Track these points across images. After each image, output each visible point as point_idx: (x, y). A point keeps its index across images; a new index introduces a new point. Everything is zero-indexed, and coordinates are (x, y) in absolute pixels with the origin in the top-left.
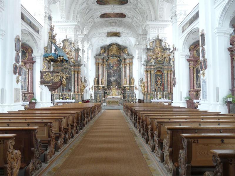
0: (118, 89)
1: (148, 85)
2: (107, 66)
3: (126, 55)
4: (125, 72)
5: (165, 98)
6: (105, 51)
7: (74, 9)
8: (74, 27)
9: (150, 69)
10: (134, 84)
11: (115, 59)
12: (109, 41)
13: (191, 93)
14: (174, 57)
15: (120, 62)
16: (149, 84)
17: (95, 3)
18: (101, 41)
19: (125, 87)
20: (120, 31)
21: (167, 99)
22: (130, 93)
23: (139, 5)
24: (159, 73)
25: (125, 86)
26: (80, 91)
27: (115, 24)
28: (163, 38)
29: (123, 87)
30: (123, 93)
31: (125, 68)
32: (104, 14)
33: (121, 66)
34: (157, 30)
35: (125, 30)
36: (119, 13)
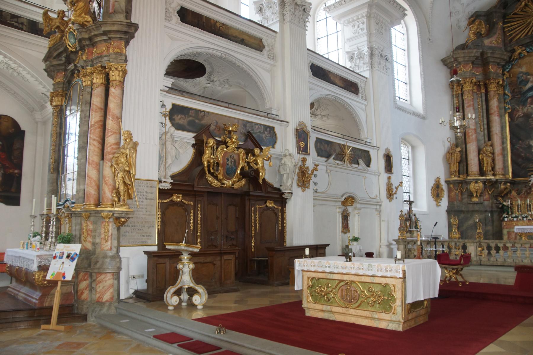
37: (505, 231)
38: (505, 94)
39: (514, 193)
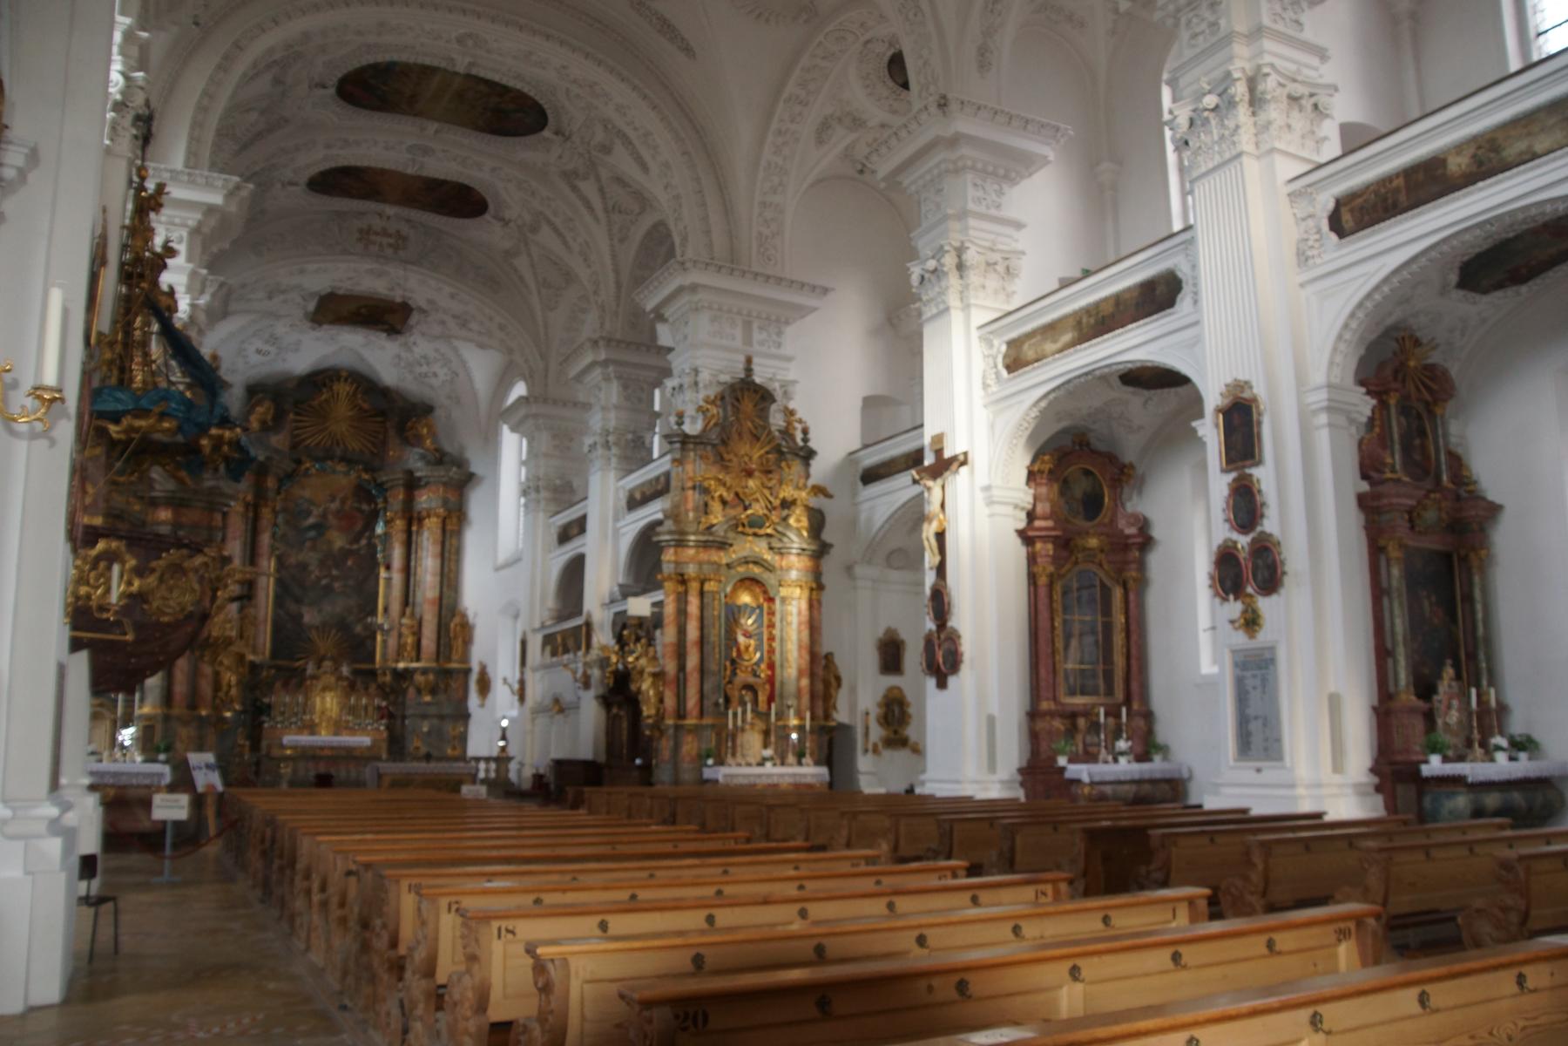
0: (352, 687)
1: (682, 668)
2: (280, 519)
3: (423, 457)
4: (407, 570)
5: (791, 758)
6: (279, 417)
7: (205, 93)
8: (191, 223)
9: (700, 564)
10: (465, 658)
11: (343, 479)
12: (310, 350)
13: (1041, 725)
14: (943, 506)
15: (371, 499)
16: (692, 661)
17: (324, 87)
18: (259, 344)
19: (406, 675)
20: (419, 298)
21: (807, 760)
22: (442, 717)
23: (621, 161)
24: (745, 598)
25: (406, 670)
26: (206, 688)
27: (396, 248)
28: (777, 385)
29: (395, 672)
30: (391, 716)
31: (409, 545)
32: (346, 171)
33: (380, 529)
34: (738, 332)
35: (452, 296)
36: (444, 182)
37: (264, 743)
38: (275, 525)
39: (278, 685)
